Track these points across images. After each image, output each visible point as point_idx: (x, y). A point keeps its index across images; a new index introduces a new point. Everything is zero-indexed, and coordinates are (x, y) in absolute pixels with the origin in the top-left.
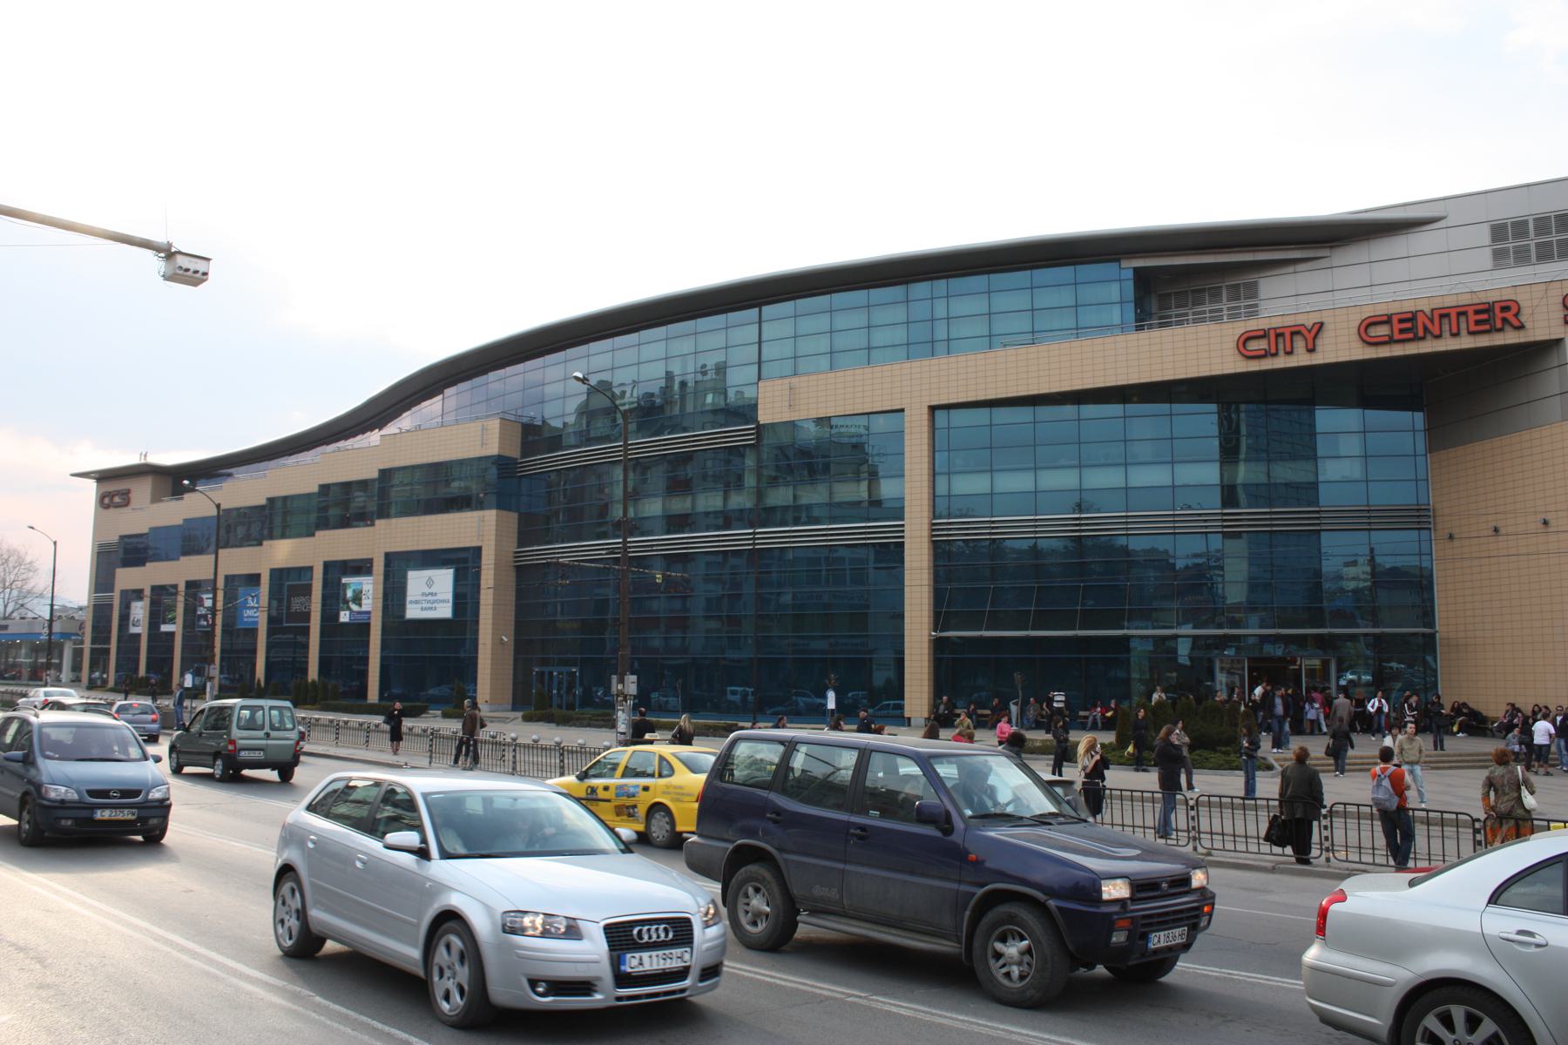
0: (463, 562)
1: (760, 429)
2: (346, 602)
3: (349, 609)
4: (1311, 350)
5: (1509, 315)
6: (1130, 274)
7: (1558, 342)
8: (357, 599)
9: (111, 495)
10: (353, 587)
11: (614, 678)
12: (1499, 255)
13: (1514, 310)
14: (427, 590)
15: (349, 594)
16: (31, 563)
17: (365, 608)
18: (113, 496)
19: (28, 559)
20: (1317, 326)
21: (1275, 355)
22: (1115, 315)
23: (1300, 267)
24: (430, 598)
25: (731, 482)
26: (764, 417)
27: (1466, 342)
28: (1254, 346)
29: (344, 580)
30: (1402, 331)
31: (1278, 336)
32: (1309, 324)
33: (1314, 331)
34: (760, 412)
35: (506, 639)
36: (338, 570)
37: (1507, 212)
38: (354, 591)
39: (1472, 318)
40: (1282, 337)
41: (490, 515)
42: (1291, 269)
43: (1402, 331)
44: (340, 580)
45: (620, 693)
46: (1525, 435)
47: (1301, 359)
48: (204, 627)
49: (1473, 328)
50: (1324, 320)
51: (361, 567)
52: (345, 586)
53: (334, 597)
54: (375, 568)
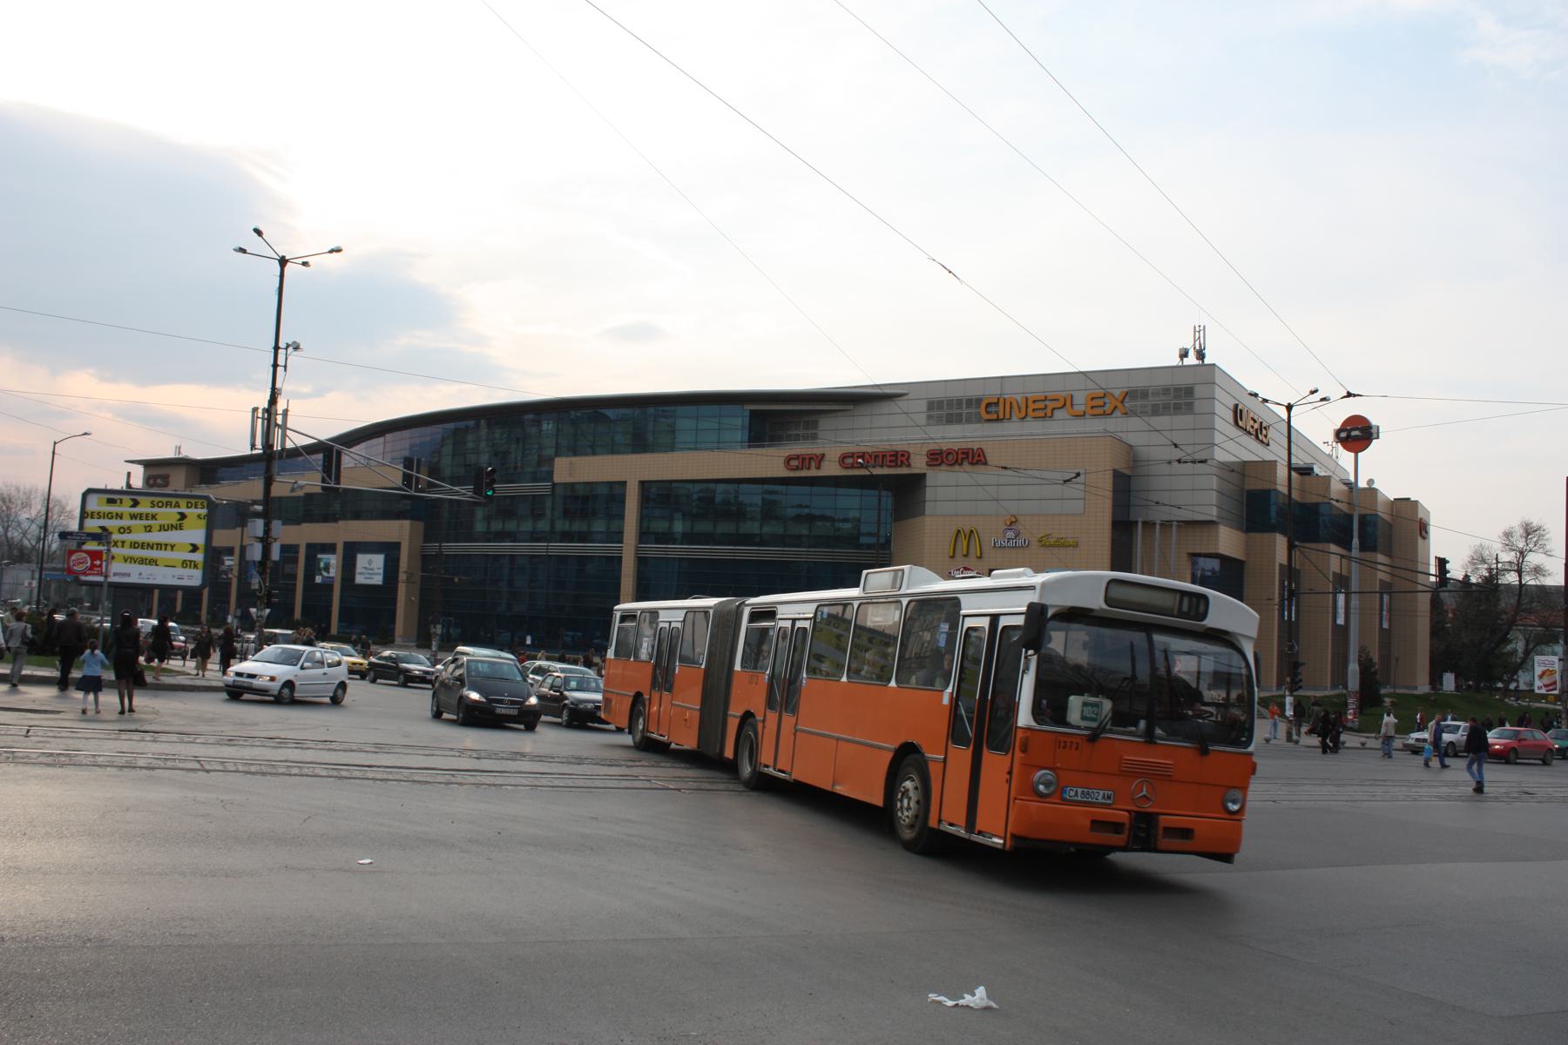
0: (390, 550)
1: (554, 485)
2: (320, 570)
3: (321, 574)
4: (818, 468)
6: (747, 413)
7: (924, 475)
8: (327, 568)
9: (155, 478)
10: (325, 561)
11: (432, 626)
12: (929, 417)
14: (368, 566)
15: (322, 565)
16: (70, 512)
17: (332, 575)
19: (68, 508)
21: (802, 469)
22: (738, 436)
23: (839, 414)
24: (370, 571)
25: (537, 515)
26: (557, 479)
27: (885, 471)
28: (794, 463)
29: (319, 556)
31: (804, 459)
35: (413, 599)
36: (315, 549)
37: (939, 394)
38: (325, 563)
39: (888, 459)
40: (805, 461)
41: (407, 523)
44: (316, 557)
45: (434, 633)
46: (918, 518)
47: (813, 473)
50: (826, 453)
51: (330, 548)
52: (320, 560)
53: (312, 567)
54: (338, 550)
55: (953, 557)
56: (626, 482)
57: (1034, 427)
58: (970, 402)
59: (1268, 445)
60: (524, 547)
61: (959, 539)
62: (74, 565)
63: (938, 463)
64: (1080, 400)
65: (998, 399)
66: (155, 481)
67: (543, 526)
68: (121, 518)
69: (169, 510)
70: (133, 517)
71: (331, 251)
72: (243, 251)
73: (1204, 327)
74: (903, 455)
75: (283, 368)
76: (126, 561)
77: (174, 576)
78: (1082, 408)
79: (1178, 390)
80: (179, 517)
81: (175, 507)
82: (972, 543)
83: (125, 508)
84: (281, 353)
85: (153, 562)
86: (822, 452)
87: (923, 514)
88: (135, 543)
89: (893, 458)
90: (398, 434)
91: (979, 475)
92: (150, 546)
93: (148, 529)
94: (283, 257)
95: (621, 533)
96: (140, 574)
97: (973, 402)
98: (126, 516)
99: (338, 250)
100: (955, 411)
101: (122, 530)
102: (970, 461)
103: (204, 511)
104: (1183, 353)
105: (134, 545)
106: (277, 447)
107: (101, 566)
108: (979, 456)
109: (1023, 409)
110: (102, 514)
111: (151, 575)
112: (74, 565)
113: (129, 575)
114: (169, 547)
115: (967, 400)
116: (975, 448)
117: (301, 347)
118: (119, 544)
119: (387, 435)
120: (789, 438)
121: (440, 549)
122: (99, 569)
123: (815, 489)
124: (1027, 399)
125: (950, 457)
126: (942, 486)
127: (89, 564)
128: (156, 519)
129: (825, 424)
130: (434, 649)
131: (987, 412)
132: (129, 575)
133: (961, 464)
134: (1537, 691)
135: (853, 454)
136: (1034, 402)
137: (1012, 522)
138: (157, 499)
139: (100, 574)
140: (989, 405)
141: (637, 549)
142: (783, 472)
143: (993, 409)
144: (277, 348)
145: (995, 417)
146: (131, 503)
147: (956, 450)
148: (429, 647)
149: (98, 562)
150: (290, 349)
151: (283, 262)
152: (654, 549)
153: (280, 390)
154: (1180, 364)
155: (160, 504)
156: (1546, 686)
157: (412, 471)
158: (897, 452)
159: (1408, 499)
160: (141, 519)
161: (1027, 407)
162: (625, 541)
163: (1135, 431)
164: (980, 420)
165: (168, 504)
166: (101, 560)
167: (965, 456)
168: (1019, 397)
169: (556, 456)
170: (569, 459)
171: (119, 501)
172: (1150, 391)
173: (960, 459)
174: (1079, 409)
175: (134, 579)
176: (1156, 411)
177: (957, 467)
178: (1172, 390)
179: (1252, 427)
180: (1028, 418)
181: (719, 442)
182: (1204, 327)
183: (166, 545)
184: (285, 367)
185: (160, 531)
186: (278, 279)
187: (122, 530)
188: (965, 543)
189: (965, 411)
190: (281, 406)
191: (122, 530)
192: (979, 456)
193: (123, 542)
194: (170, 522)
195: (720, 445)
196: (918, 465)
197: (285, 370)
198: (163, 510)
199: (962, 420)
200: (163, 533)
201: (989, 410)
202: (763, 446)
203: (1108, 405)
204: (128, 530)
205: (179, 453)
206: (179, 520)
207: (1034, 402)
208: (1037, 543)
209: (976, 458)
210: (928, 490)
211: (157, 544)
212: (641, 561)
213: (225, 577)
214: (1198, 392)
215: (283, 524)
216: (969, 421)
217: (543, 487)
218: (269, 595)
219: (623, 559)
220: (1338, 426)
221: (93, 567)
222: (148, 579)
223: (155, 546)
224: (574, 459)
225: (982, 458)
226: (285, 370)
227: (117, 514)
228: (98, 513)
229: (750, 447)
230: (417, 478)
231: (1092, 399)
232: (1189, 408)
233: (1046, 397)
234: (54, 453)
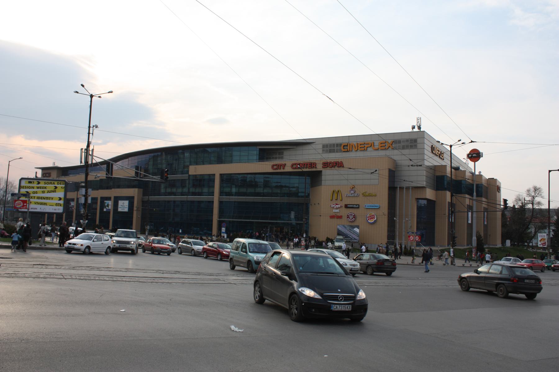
0: (130, 199)
1: (189, 175)
2: (105, 206)
3: (106, 208)
4: (284, 169)
5: (314, 165)
6: (258, 149)
8: (108, 206)
9: (46, 174)
10: (107, 203)
11: (146, 226)
12: (323, 150)
13: (315, 164)
14: (122, 205)
15: (106, 205)
16: (15, 186)
17: (110, 208)
18: (47, 174)
19: (14, 185)
21: (278, 169)
22: (256, 158)
23: (291, 150)
24: (123, 207)
25: (183, 186)
26: (190, 173)
28: (275, 167)
29: (105, 201)
34: (189, 172)
35: (139, 216)
36: (103, 199)
38: (107, 204)
40: (279, 166)
41: (136, 190)
42: (289, 150)
47: (282, 170)
48: (71, 210)
49: (309, 167)
51: (109, 199)
52: (105, 203)
53: (103, 205)
55: (332, 200)
56: (215, 174)
57: (360, 154)
58: (337, 145)
59: (444, 159)
60: (178, 198)
61: (334, 194)
62: (17, 205)
63: (326, 167)
64: (377, 143)
65: (348, 144)
66: (46, 175)
67: (186, 190)
68: (34, 188)
69: (51, 185)
70: (38, 188)
71: (109, 92)
72: (77, 92)
73: (421, 118)
74: (314, 164)
75: (92, 134)
76: (35, 204)
77: (53, 209)
78: (377, 147)
79: (411, 140)
80: (54, 188)
81: (53, 184)
82: (339, 195)
83: (35, 185)
84: (91, 129)
85: (45, 204)
86: (285, 163)
87: (321, 185)
88: (39, 197)
89: (310, 165)
90: (133, 158)
91: (341, 171)
92: (44, 198)
93: (43, 192)
94: (92, 95)
95: (213, 192)
96: (41, 208)
97: (339, 145)
98: (35, 187)
99: (111, 92)
100: (332, 148)
101: (34, 193)
103: (64, 186)
104: (413, 127)
105: (38, 198)
106: (90, 162)
107: (26, 205)
108: (341, 164)
109: (357, 148)
110: (27, 187)
111: (44, 209)
112: (17, 205)
113: (36, 209)
114: (51, 199)
115: (337, 144)
117: (98, 127)
118: (33, 198)
119: (129, 158)
120: (273, 158)
121: (148, 199)
122: (26, 207)
123: (283, 176)
124: (358, 144)
125: (331, 165)
126: (328, 175)
127: (22, 205)
128: (46, 189)
129: (286, 153)
130: (147, 234)
131: (344, 149)
132: (36, 209)
133: (334, 167)
134: (539, 246)
135: (296, 164)
136: (360, 145)
137: (353, 188)
138: (46, 182)
139: (26, 208)
140: (344, 146)
141: (219, 198)
142: (271, 171)
143: (346, 147)
144: (89, 127)
145: (346, 150)
146: (37, 183)
147: (333, 161)
148: (145, 234)
149: (25, 204)
150: (94, 127)
151: (92, 96)
152: (225, 198)
153: (91, 142)
154: (412, 131)
155: (48, 183)
156: (542, 244)
157: (138, 171)
158: (312, 163)
159: (493, 178)
160: (41, 189)
161: (358, 147)
162: (215, 195)
163: (396, 155)
164: (341, 151)
165: (51, 183)
166: (26, 203)
167: (336, 164)
168: (355, 143)
169: (190, 165)
170: (194, 166)
171: (33, 182)
172: (402, 141)
173: (334, 165)
174: (377, 147)
175: (38, 210)
176: (403, 148)
177: (333, 168)
178: (409, 141)
179: (438, 153)
180: (358, 151)
181: (248, 160)
182: (421, 118)
183: (50, 198)
184: (93, 134)
185: (48, 193)
186: (90, 102)
187: (34, 193)
188: (336, 195)
189: (336, 148)
190: (91, 148)
191: (34, 193)
193: (34, 197)
194: (51, 190)
195: (248, 161)
196: (319, 167)
197: (93, 135)
198: (49, 185)
199: (335, 152)
200: (49, 193)
201: (344, 148)
202: (264, 161)
203: (386, 146)
204: (36, 192)
205: (54, 165)
206: (55, 189)
207: (360, 145)
208: (362, 195)
209: (340, 165)
210: (323, 176)
211: (47, 198)
212: (221, 203)
213: (71, 209)
214: (419, 141)
215: (92, 190)
216: (337, 152)
217: (185, 176)
218: (87, 216)
219: (214, 202)
220: (468, 153)
221: (23, 206)
222: (43, 210)
223: (46, 198)
224: (196, 166)
225: (342, 165)
226: (93, 135)
227: (32, 187)
228: (25, 187)
229: (259, 161)
230: (140, 173)
231: (381, 144)
232: (415, 147)
233: (365, 143)
234: (9, 165)
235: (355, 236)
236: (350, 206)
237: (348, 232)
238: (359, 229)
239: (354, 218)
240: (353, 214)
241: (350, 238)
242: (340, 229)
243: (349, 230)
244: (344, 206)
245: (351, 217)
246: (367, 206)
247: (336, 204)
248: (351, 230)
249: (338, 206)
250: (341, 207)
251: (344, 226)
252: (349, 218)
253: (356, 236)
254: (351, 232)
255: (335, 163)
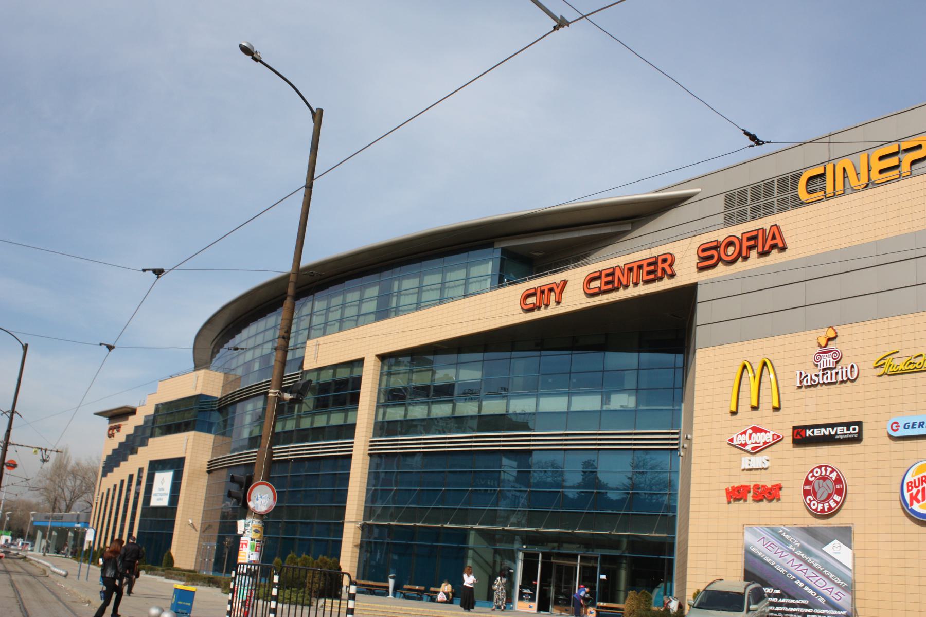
4: (558, 303)
5: (666, 266)
20: (562, 283)
21: (539, 308)
30: (607, 283)
32: (558, 281)
33: (560, 288)
39: (646, 269)
43: (607, 283)
55: (734, 413)
74: (664, 261)
102: (760, 250)
108: (774, 238)
116: (767, 228)
125: (731, 250)
131: (809, 192)
137: (829, 340)
143: (818, 183)
158: (657, 258)
167: (752, 243)
188: (754, 385)
192: (774, 238)
225: (778, 241)
235: (829, 585)
236: (817, 432)
237: (797, 562)
238: (850, 548)
239: (839, 492)
240: (834, 476)
241: (807, 596)
242: (753, 550)
243: (799, 553)
244: (788, 439)
245: (823, 489)
246: (902, 425)
247: (756, 430)
248: (808, 553)
249: (760, 438)
250: (778, 440)
251: (773, 530)
252: (815, 494)
253: (836, 590)
254: (811, 566)
255: (749, 239)
